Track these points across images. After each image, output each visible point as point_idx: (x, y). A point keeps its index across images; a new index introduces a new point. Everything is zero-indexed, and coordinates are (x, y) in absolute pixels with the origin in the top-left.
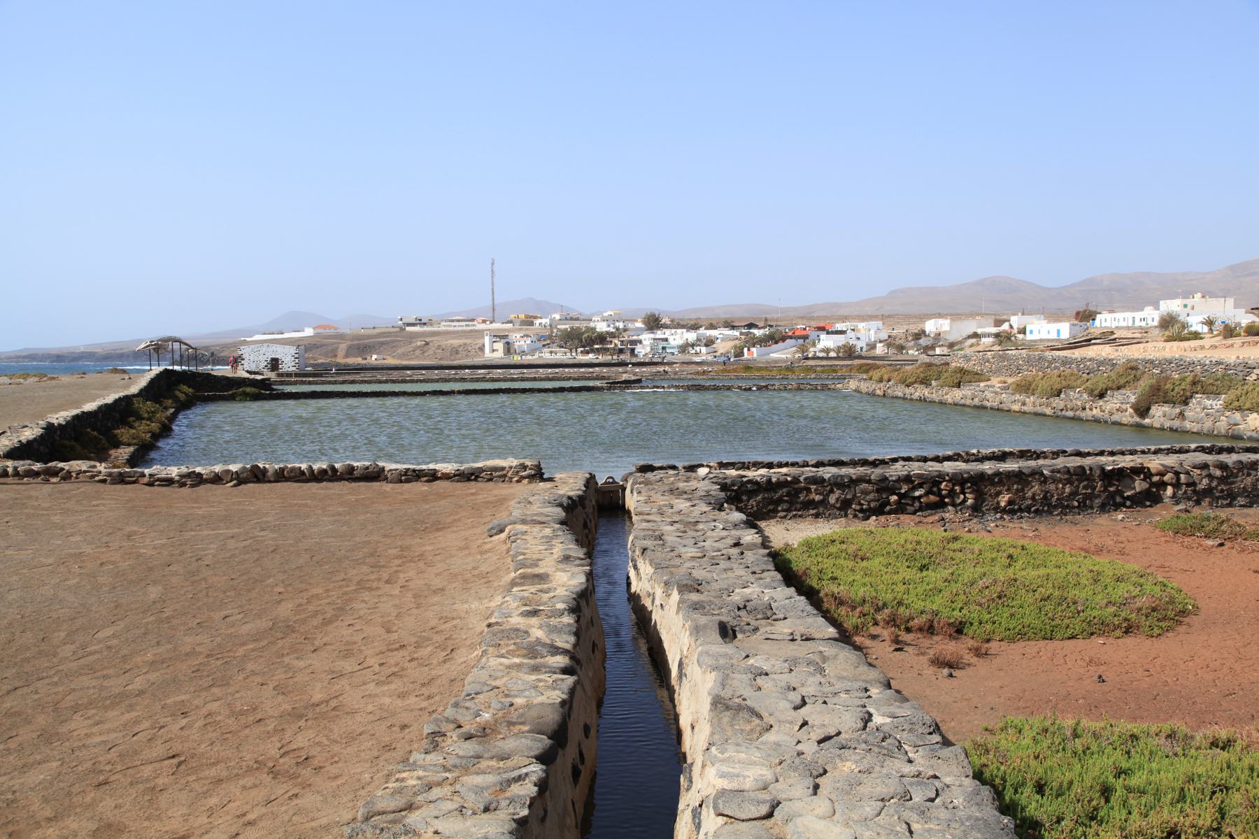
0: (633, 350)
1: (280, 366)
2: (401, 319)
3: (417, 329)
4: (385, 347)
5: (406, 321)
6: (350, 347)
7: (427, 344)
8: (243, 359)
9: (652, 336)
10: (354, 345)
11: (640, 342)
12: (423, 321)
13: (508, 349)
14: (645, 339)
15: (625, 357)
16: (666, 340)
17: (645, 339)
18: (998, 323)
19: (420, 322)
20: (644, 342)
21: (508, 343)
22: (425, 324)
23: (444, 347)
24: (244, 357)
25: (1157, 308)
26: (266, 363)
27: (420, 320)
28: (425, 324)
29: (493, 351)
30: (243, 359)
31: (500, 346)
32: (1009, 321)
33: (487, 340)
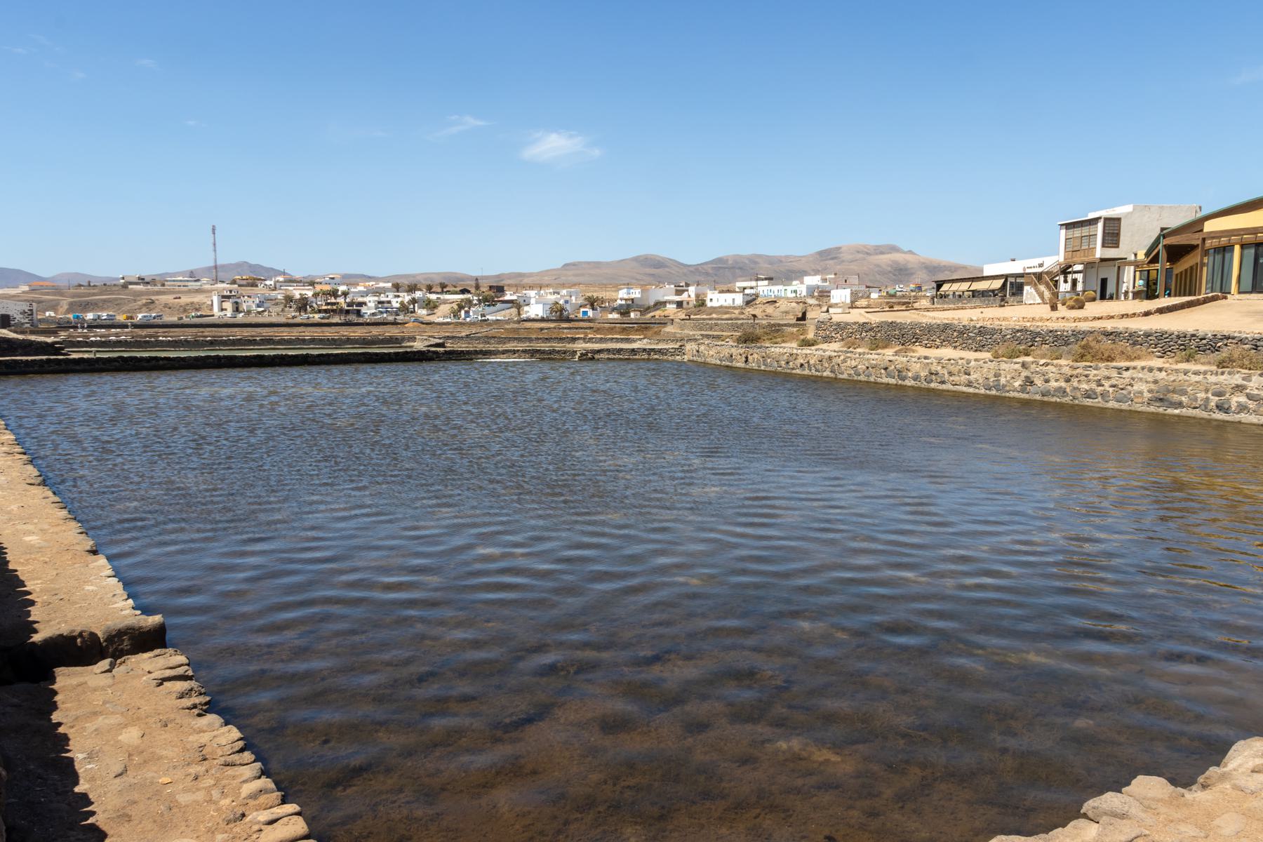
0: (358, 313)
2: (123, 278)
3: (140, 287)
4: (109, 304)
5: (127, 279)
6: (71, 304)
7: (153, 302)
9: (376, 298)
10: (75, 302)
11: (365, 304)
12: (147, 280)
13: (237, 309)
14: (370, 302)
15: (353, 318)
16: (389, 302)
17: (370, 302)
18: (679, 293)
19: (142, 280)
20: (369, 304)
21: (237, 303)
22: (148, 283)
23: (171, 305)
25: (802, 283)
27: (143, 279)
28: (148, 283)
29: (222, 310)
31: (228, 305)
32: (687, 291)
33: (215, 299)
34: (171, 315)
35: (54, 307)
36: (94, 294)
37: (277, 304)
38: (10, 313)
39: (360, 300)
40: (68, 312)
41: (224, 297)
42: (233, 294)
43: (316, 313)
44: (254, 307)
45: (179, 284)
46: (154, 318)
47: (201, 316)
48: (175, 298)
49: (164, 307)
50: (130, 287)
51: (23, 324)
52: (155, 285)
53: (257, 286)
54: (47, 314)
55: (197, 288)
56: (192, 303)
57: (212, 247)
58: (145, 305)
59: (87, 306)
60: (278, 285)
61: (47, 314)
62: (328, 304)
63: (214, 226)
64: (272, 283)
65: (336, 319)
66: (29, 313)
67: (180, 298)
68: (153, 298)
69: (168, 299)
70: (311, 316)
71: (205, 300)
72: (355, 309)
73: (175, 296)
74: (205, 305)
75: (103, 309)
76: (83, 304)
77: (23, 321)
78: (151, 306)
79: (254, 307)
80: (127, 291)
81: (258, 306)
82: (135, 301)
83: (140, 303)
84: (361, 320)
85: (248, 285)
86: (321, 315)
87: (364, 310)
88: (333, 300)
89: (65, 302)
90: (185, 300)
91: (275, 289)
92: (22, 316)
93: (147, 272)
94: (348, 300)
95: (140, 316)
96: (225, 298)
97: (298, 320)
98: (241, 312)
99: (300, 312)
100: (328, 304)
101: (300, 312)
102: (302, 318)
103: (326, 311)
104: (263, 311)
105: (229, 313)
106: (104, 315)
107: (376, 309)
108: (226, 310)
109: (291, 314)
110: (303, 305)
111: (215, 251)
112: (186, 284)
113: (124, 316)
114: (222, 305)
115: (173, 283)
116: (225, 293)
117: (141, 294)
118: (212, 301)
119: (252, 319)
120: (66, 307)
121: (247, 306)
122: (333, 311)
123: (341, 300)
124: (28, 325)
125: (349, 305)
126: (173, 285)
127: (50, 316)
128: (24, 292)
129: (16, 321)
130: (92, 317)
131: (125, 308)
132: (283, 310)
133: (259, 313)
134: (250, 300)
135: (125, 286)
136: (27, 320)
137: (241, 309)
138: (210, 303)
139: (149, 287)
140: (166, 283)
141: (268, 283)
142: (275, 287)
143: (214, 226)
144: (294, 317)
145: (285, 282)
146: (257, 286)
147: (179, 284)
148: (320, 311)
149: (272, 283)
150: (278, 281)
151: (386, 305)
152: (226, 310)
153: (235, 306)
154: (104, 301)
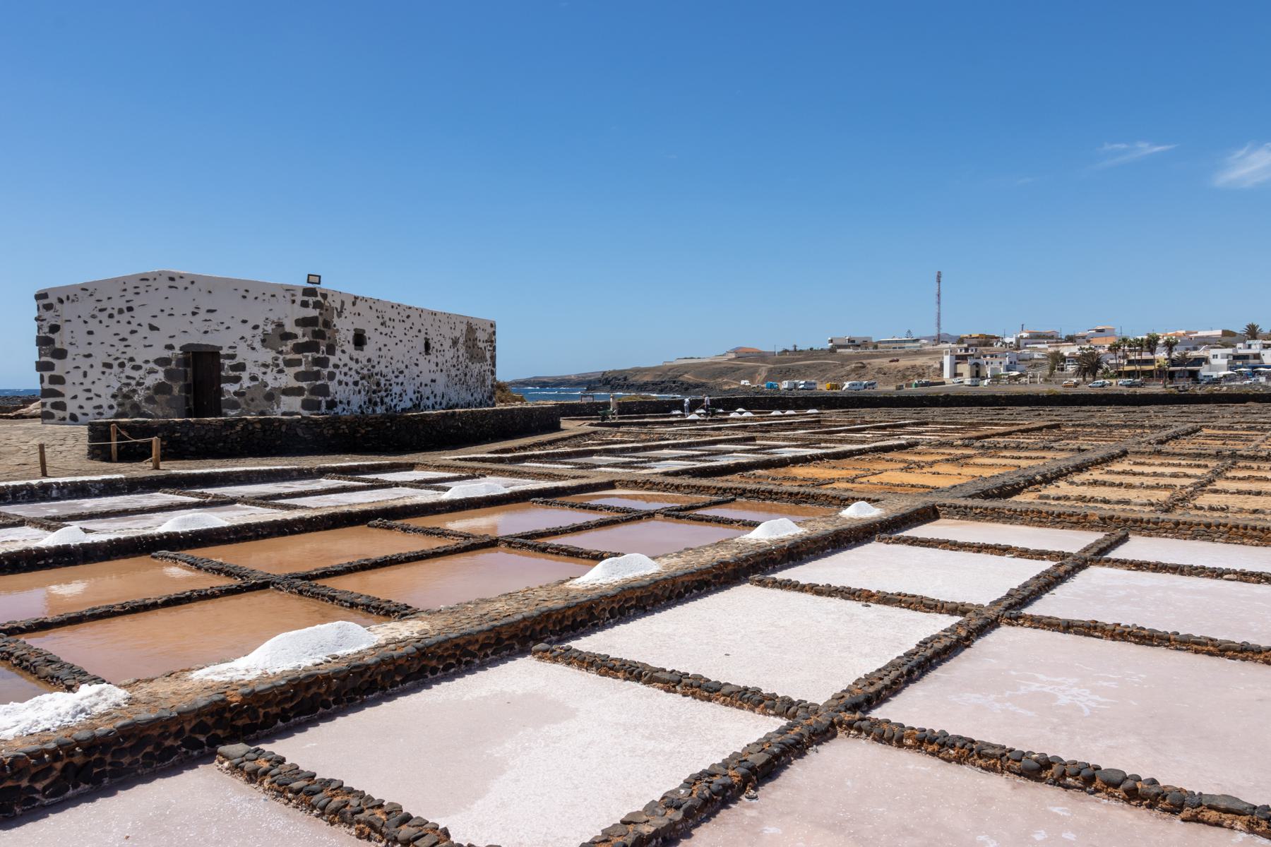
0: (1194, 375)
1: (230, 388)
2: (831, 341)
3: (850, 351)
6: (770, 371)
7: (864, 367)
8: (61, 354)
9: (1229, 351)
10: (775, 368)
11: (1204, 360)
12: (857, 343)
13: (977, 374)
14: (1215, 356)
15: (1185, 385)
16: (1257, 356)
19: (852, 341)
20: (1214, 362)
21: (977, 365)
22: (859, 346)
23: (886, 370)
24: (60, 340)
26: (160, 376)
27: (854, 341)
28: (859, 346)
29: (956, 375)
30: (61, 354)
31: (965, 368)
33: (947, 360)
34: (887, 383)
35: (751, 375)
36: (798, 360)
37: (1035, 366)
38: (221, 340)
39: (1195, 354)
40: (764, 381)
41: (958, 357)
42: (970, 352)
43: (1112, 377)
44: (1002, 371)
45: (894, 345)
46: (865, 387)
47: (927, 384)
48: (891, 361)
49: (877, 372)
50: (839, 351)
51: (270, 397)
52: (866, 348)
53: (992, 345)
54: (743, 382)
55: (915, 349)
56: (913, 367)
57: (935, 299)
58: (853, 370)
59: (786, 373)
60: (1022, 342)
61: (743, 382)
62: (1130, 362)
63: (939, 272)
64: (1013, 340)
65: (1156, 388)
66: (303, 336)
67: (898, 361)
68: (864, 362)
69: (884, 362)
70: (1107, 382)
71: (931, 363)
72: (1188, 368)
73: (890, 359)
74: (931, 370)
75: (803, 376)
76: (784, 371)
77: (273, 381)
78: (862, 372)
79: (1002, 371)
80: (835, 356)
81: (1008, 369)
82: (843, 366)
83: (848, 368)
84: (1199, 390)
85: (980, 345)
86: (1128, 380)
87: (1204, 371)
88: (1146, 356)
89: (764, 368)
90: (904, 363)
91: (1018, 347)
92: (267, 355)
93: (859, 334)
94: (1175, 354)
95: (847, 385)
96: (960, 359)
97: (1084, 389)
98: (983, 378)
99: (1084, 376)
100: (1130, 362)
101: (1084, 376)
102: (1089, 387)
103: (1129, 374)
104: (1019, 376)
105: (967, 381)
106: (801, 383)
107: (1230, 368)
108: (961, 375)
109: (1070, 380)
110: (1090, 365)
111: (939, 303)
112: (903, 345)
113: (828, 385)
114: (956, 369)
115: (887, 345)
116: (959, 353)
117: (849, 358)
118: (942, 365)
119: (1003, 389)
120: (764, 374)
121: (991, 369)
122: (1144, 373)
123: (1161, 355)
124: (293, 404)
125: (1173, 362)
126: (887, 348)
127: (744, 386)
128: (730, 360)
129: (246, 382)
130: (786, 386)
131: (830, 375)
132: (1051, 374)
133: (1016, 378)
134: (996, 361)
135: (832, 350)
136: (288, 379)
137: (982, 374)
138: (938, 366)
139: (860, 350)
140: (879, 345)
141: (1007, 340)
142: (1019, 346)
143: (939, 272)
144: (1077, 385)
145: (1031, 338)
146: (992, 345)
147: (894, 345)
148: (1119, 374)
149: (1013, 340)
150: (1022, 337)
151: (1252, 362)
152: (961, 375)
153: (975, 369)
154: (808, 366)
